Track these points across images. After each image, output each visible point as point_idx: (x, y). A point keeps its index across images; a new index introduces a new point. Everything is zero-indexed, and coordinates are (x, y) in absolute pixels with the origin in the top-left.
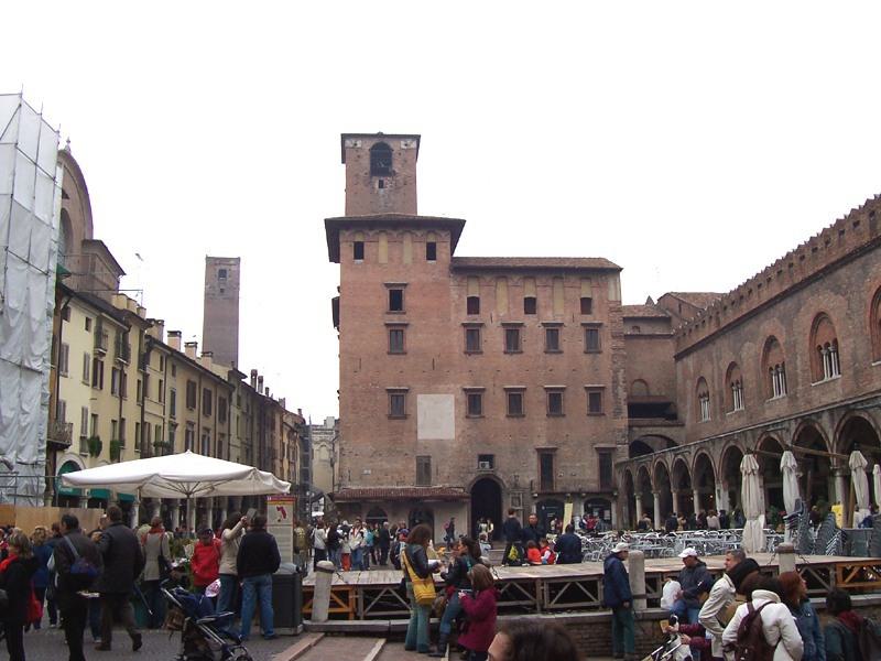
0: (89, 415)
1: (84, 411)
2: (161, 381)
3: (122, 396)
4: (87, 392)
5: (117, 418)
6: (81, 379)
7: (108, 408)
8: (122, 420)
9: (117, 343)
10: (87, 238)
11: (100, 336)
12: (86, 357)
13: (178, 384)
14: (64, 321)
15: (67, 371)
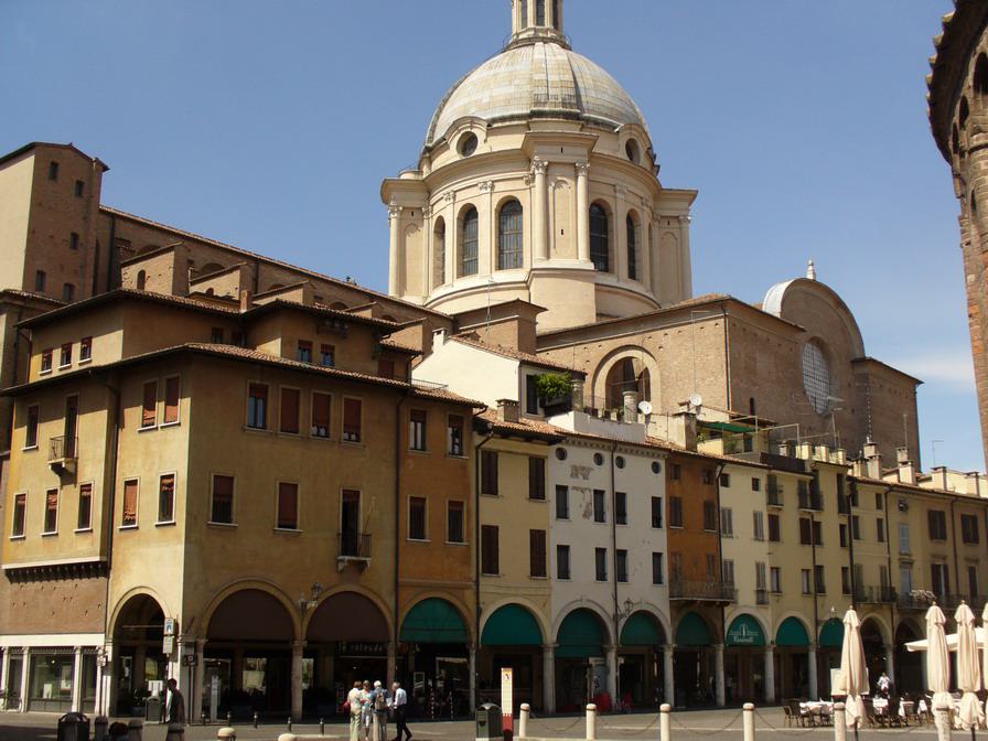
0: (768, 571)
1: (760, 567)
2: (879, 521)
3: (818, 541)
4: (762, 551)
5: (811, 567)
6: (752, 536)
7: (793, 556)
8: (819, 569)
9: (801, 494)
10: (858, 356)
11: (773, 494)
12: (757, 517)
13: (917, 522)
14: (722, 489)
15: (731, 532)
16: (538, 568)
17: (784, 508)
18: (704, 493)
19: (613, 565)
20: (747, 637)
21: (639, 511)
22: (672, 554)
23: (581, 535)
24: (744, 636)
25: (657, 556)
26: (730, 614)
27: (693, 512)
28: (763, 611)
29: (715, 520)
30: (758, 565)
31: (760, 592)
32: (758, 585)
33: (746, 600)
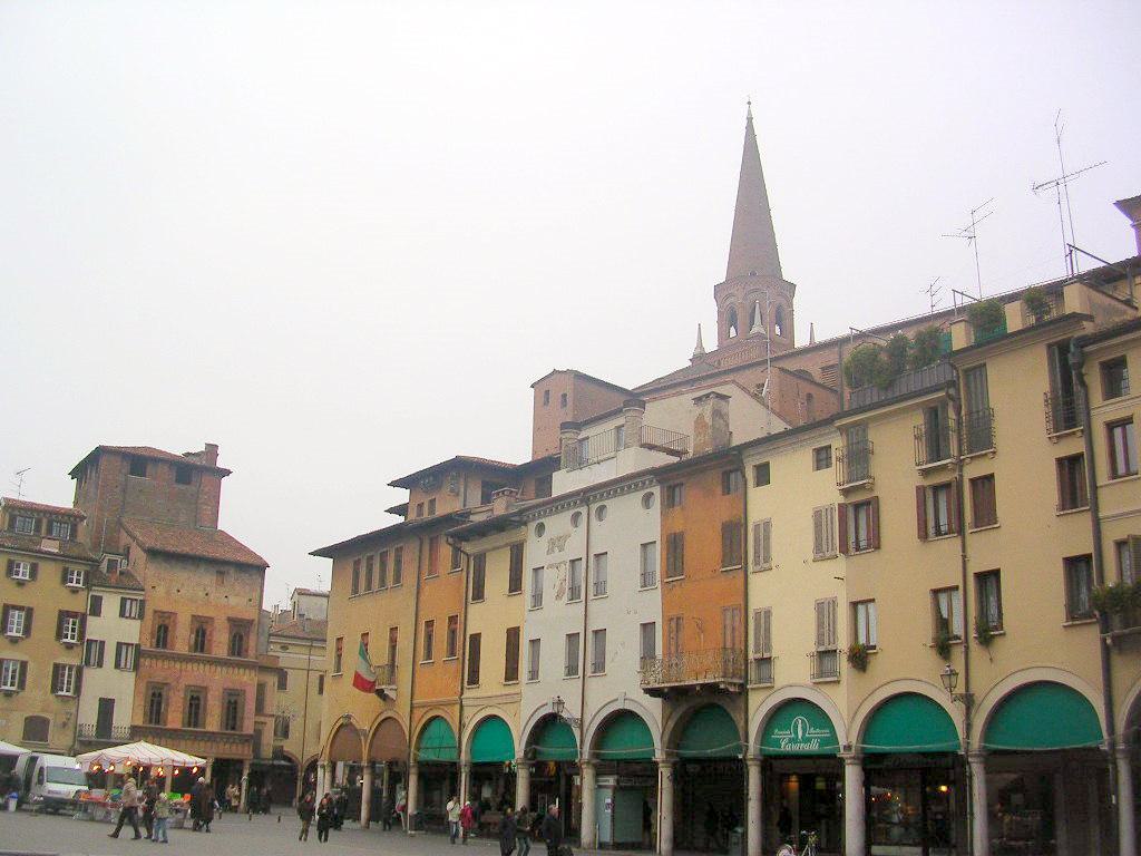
1: (824, 610)
4: (833, 579)
7: (910, 572)
16: (511, 673)
17: (878, 482)
18: (723, 510)
19: (586, 653)
20: (808, 740)
21: (623, 570)
22: (668, 620)
23: (551, 623)
24: (797, 739)
25: (648, 628)
26: (759, 706)
27: (704, 547)
28: (827, 689)
29: (738, 546)
30: (820, 606)
31: (825, 655)
32: (820, 642)
33: (792, 673)
